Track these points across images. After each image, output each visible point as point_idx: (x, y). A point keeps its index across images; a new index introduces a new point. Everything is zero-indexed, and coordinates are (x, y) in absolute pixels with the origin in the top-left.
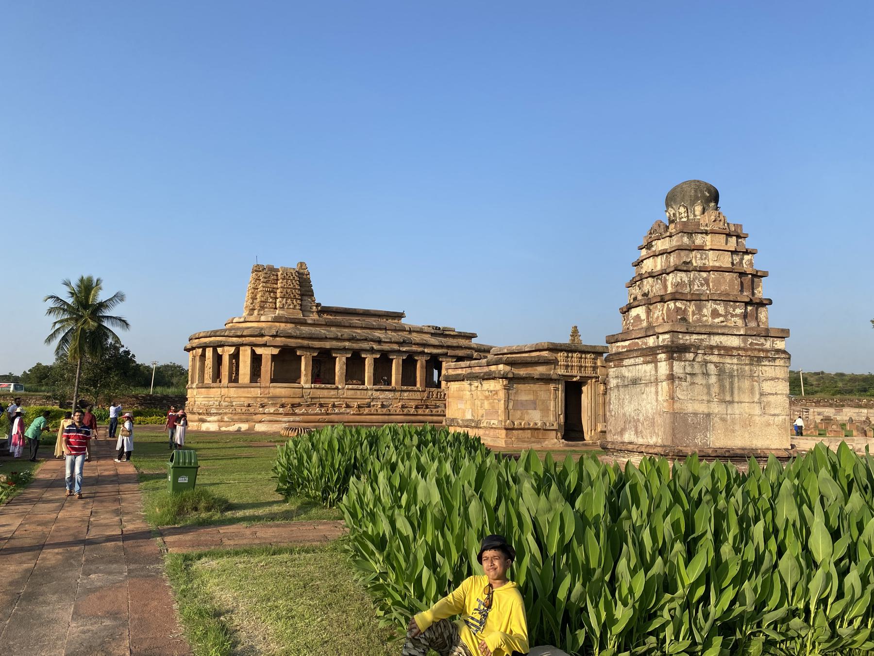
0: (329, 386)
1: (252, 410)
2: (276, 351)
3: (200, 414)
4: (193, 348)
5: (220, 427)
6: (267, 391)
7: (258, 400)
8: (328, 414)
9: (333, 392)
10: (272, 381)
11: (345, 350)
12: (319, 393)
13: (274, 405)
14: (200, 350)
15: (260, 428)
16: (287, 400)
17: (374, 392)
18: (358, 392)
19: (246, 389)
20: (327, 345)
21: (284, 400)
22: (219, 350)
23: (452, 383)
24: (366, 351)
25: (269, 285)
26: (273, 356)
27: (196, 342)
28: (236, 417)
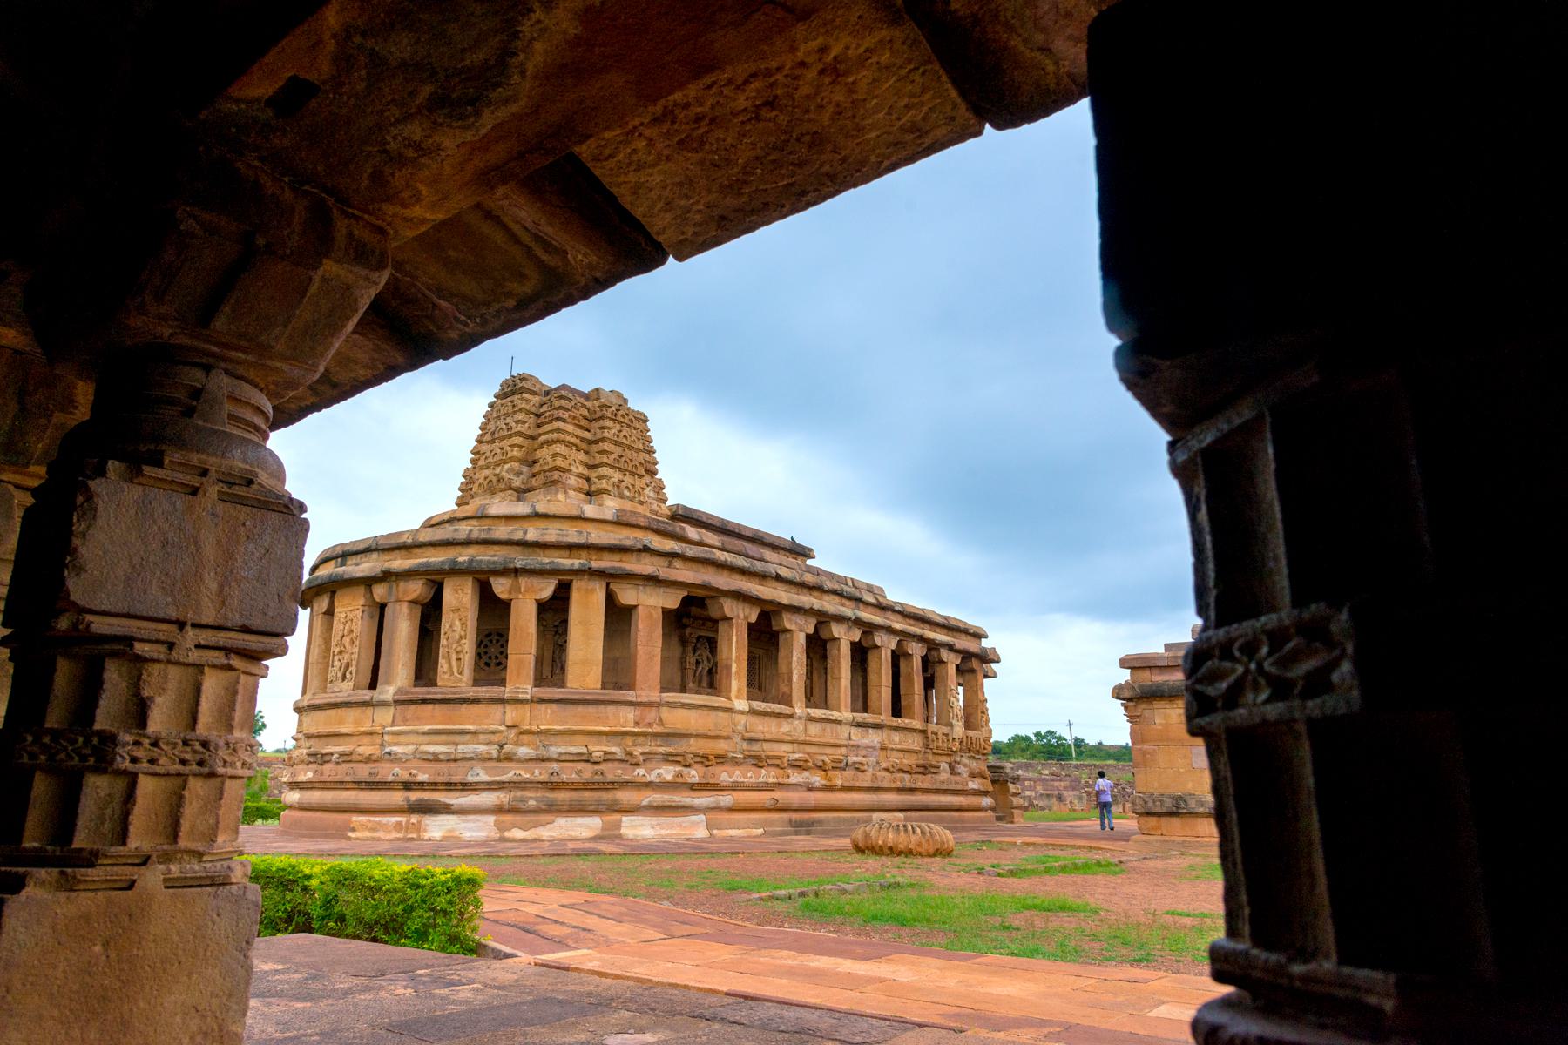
0: (777, 708)
1: (613, 772)
2: (673, 600)
3: (407, 786)
4: (386, 576)
5: (501, 827)
6: (652, 714)
7: (629, 741)
8: (780, 786)
9: (786, 727)
10: (665, 689)
11: (810, 612)
12: (762, 727)
13: (669, 758)
14: (416, 589)
15: (640, 828)
16: (701, 742)
17: (853, 730)
18: (828, 726)
19: (591, 709)
20: (784, 596)
21: (696, 746)
22: (501, 587)
23: (1157, 704)
24: (840, 619)
25: (570, 428)
26: (667, 613)
27: (398, 563)
28: (562, 796)
